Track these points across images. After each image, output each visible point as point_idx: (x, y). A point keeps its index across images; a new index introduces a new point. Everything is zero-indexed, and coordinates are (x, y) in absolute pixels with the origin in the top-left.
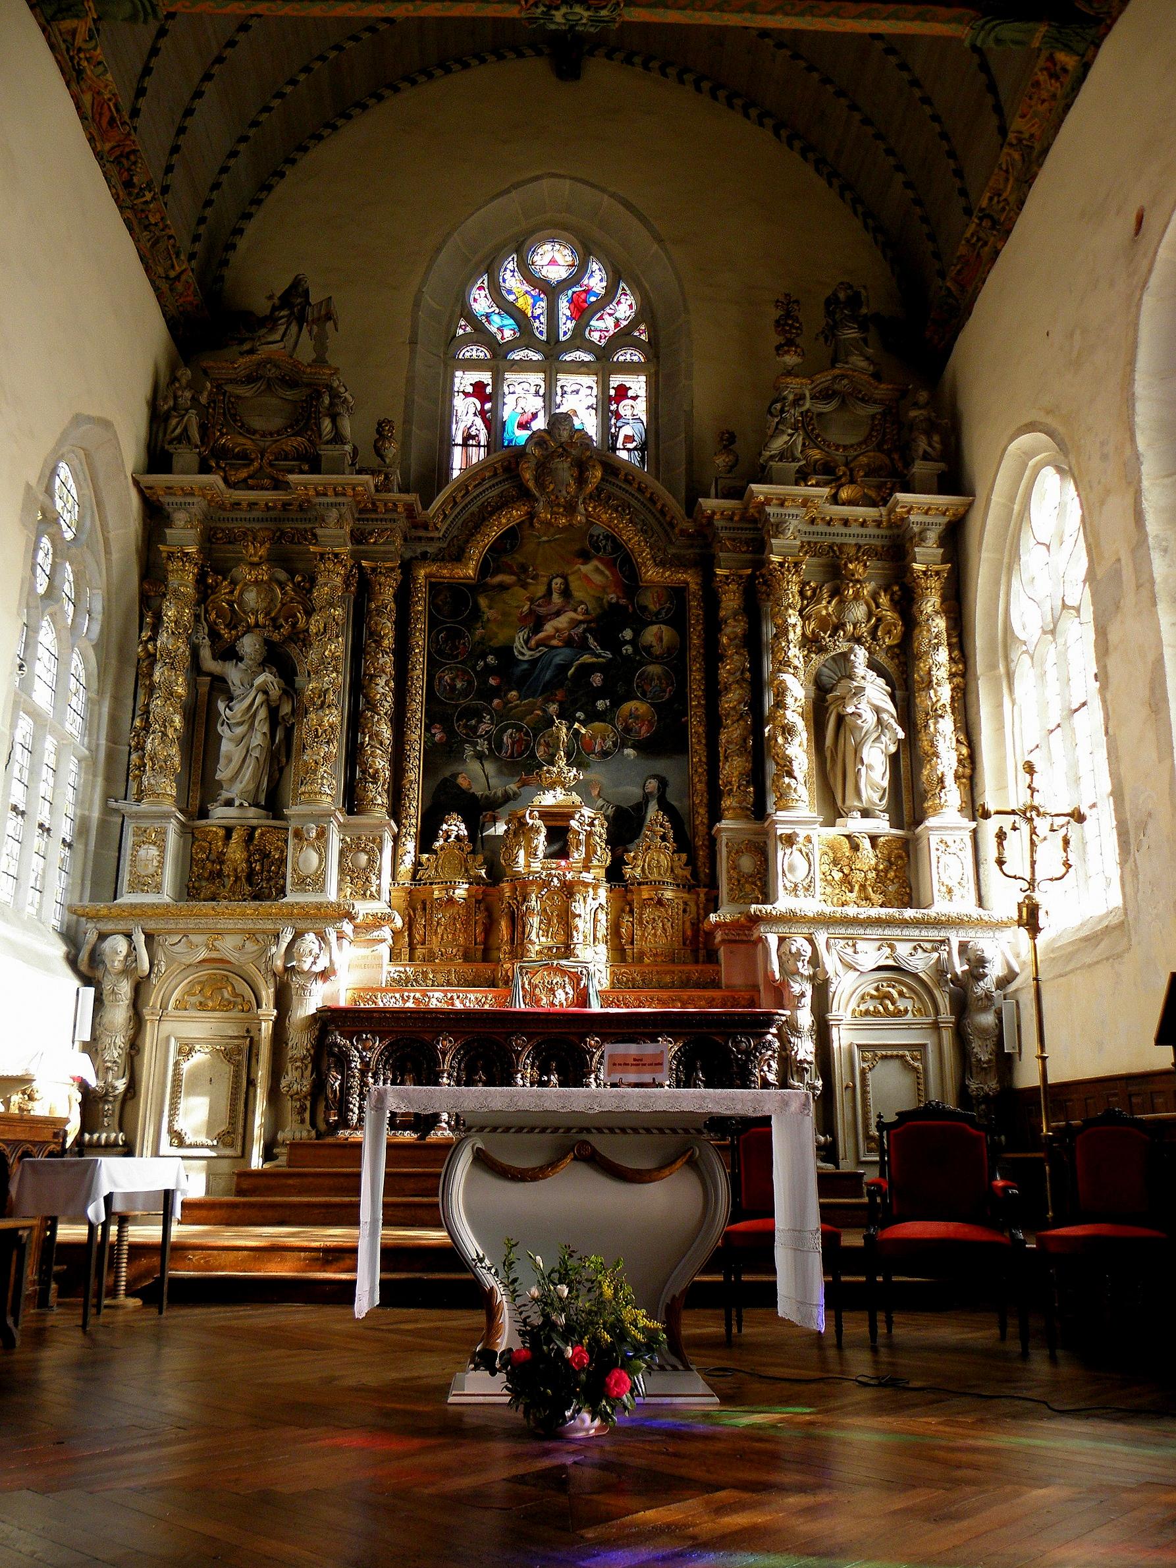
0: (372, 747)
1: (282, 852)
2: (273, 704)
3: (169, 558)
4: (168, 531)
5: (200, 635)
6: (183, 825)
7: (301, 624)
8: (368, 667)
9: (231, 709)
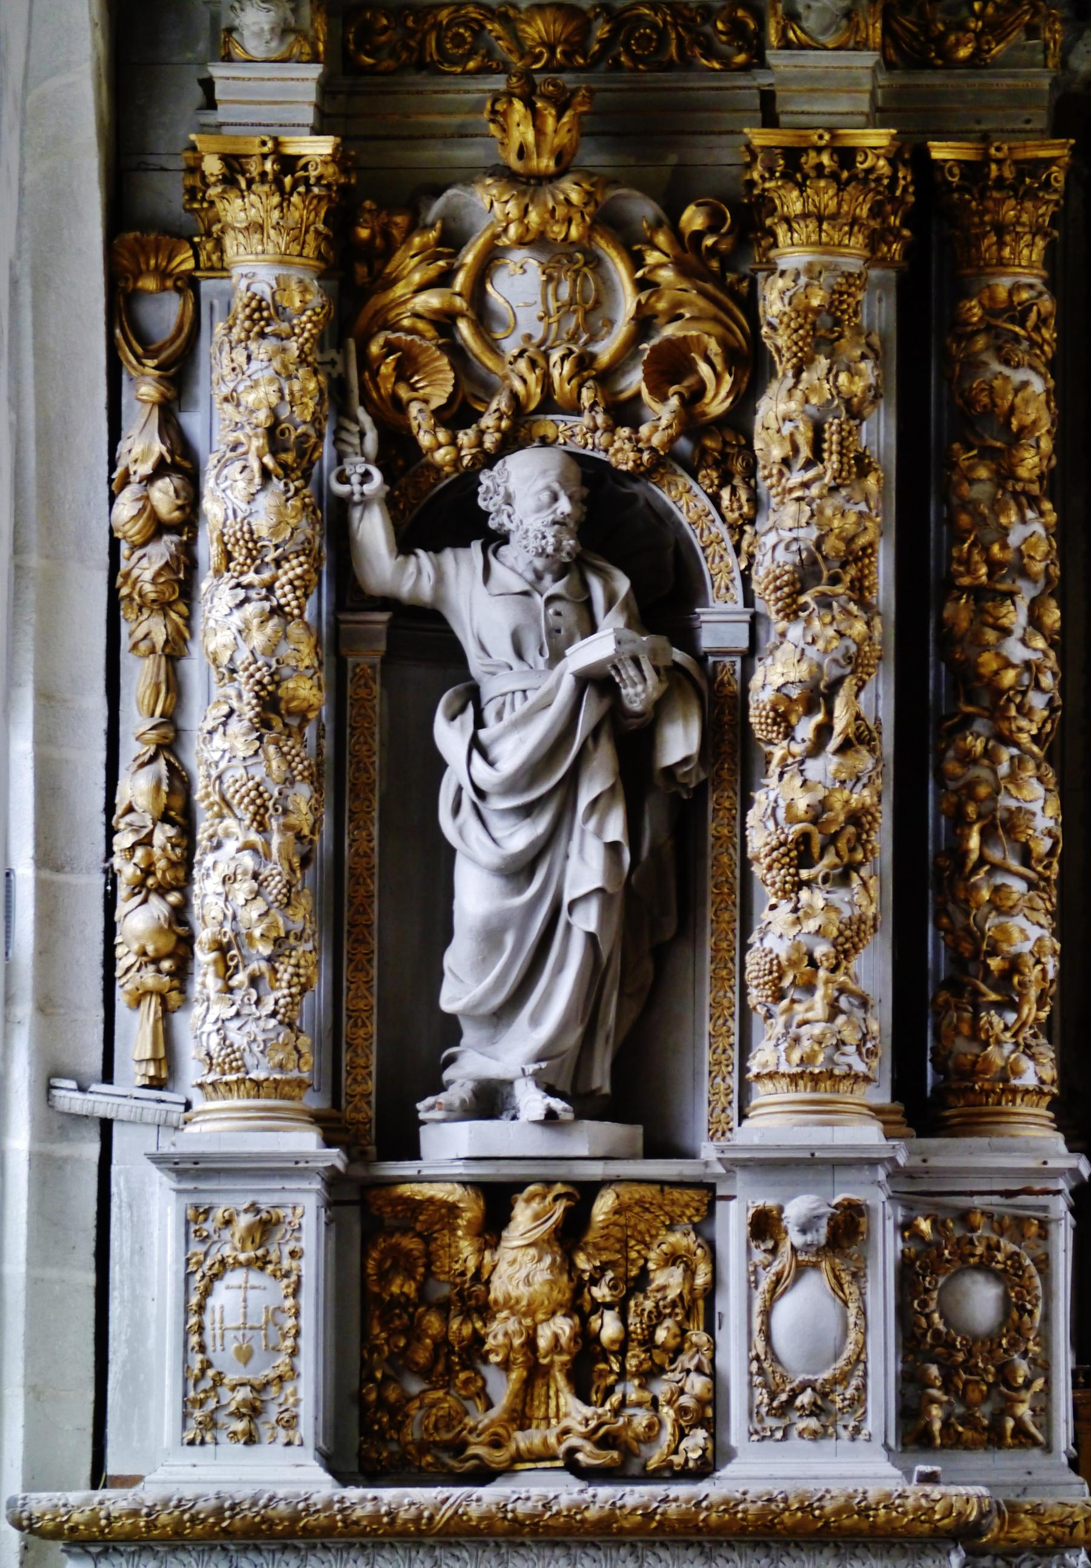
0: (996, 868)
1: (690, 1272)
2: (633, 724)
3: (229, 181)
4: (218, 71)
5: (355, 466)
6: (333, 1180)
7: (717, 403)
8: (967, 562)
9: (485, 755)
